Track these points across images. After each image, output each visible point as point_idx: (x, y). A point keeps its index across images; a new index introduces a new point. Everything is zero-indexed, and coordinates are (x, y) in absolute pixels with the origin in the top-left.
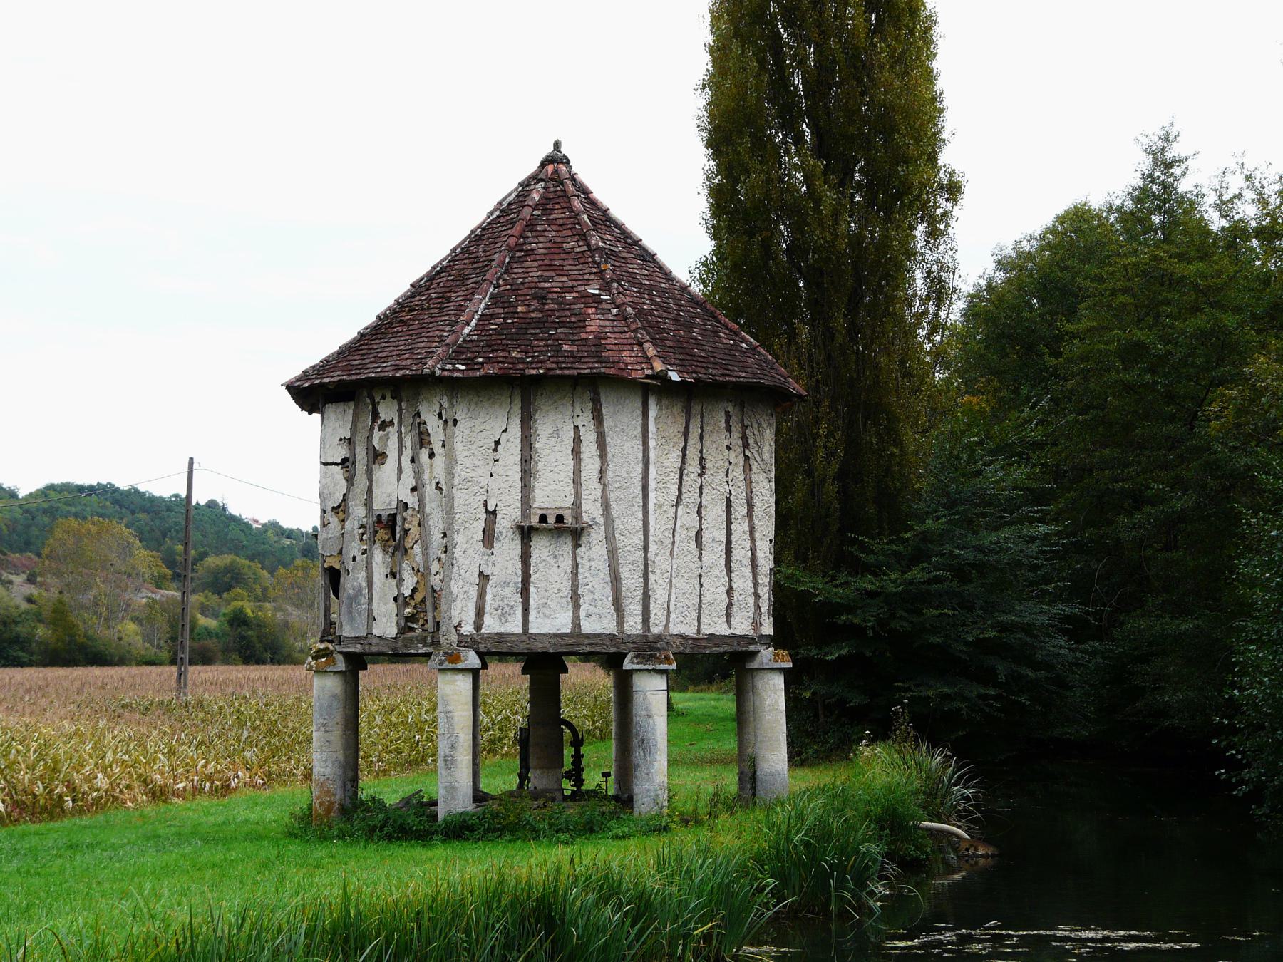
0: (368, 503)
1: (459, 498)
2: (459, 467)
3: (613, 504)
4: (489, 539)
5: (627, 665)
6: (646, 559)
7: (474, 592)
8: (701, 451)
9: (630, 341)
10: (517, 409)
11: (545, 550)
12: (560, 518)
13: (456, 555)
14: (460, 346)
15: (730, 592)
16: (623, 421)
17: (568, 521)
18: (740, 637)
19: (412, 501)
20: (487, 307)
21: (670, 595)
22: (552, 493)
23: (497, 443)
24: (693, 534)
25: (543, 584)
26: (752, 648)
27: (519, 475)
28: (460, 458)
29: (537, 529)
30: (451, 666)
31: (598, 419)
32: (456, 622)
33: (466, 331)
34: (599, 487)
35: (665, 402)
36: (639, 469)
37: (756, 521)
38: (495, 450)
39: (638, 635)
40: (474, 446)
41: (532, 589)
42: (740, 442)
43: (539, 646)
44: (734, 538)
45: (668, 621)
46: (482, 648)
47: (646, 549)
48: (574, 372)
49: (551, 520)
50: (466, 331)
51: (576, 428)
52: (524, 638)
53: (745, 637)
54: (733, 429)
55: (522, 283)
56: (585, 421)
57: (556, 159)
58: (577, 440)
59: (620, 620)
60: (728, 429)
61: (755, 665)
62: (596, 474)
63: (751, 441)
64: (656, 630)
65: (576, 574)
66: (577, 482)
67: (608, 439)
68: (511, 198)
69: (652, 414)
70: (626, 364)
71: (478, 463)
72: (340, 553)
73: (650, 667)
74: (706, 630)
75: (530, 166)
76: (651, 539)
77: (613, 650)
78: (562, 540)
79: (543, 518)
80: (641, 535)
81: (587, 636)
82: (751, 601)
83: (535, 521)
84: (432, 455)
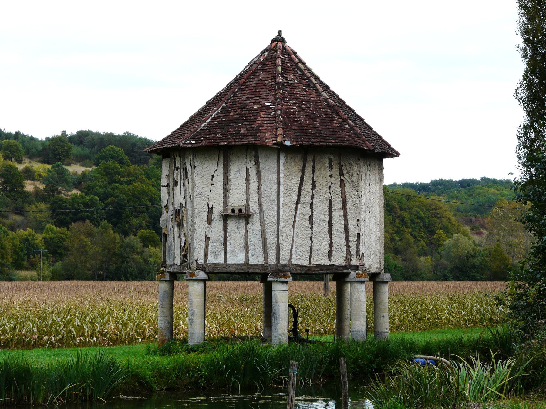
1: (197, 201)
2: (196, 188)
3: (264, 204)
4: (209, 220)
5: (269, 279)
6: (278, 229)
7: (203, 245)
8: (313, 178)
9: (273, 128)
10: (222, 161)
11: (234, 226)
12: (240, 211)
13: (196, 228)
14: (198, 132)
15: (331, 245)
16: (268, 166)
17: (244, 211)
18: (337, 266)
19: (183, 203)
20: (218, 113)
21: (292, 246)
22: (237, 199)
23: (213, 176)
24: (307, 217)
25: (233, 241)
26: (345, 271)
27: (222, 191)
28: (197, 183)
29: (230, 216)
30: (190, 278)
31: (257, 164)
32: (196, 258)
33: (203, 125)
34: (257, 196)
35: (290, 156)
36: (275, 187)
37: (348, 211)
38: (212, 179)
39: (274, 265)
40: (203, 178)
41: (228, 243)
42: (338, 173)
43: (231, 269)
44: (334, 219)
45: (291, 258)
46: (207, 270)
47: (278, 224)
48: (241, 143)
49: (237, 211)
50: (203, 125)
51: (247, 169)
52: (224, 266)
53: (340, 266)
54: (334, 167)
55: (238, 101)
56: (252, 165)
57: (279, 39)
58: (248, 174)
59: (266, 258)
60: (331, 167)
61: (348, 279)
62: (256, 189)
63: (345, 172)
64: (283, 262)
65: (247, 236)
66: (247, 193)
67: (262, 174)
68: (256, 60)
69: (282, 160)
70: (266, 139)
71: (205, 186)
72: (166, 227)
73: (275, 280)
74: (315, 262)
75: (266, 43)
76: (281, 220)
77: (263, 272)
78: (241, 221)
79: (233, 211)
80: (276, 218)
81: (252, 265)
82: (345, 249)
83: (229, 212)
84: (188, 183)
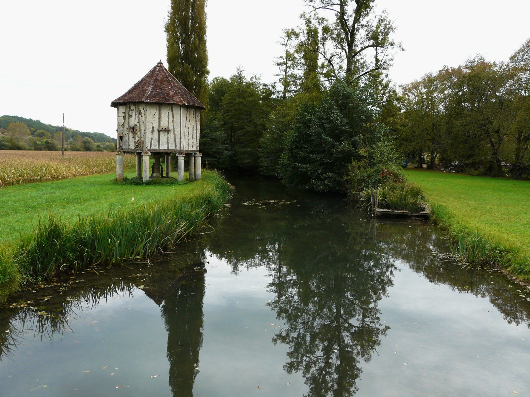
0: (128, 124)
5: (177, 155)
7: (150, 141)
16: (177, 111)
19: (138, 124)
22: (164, 124)
43: (161, 151)
56: (170, 111)
58: (169, 115)
66: (168, 122)
